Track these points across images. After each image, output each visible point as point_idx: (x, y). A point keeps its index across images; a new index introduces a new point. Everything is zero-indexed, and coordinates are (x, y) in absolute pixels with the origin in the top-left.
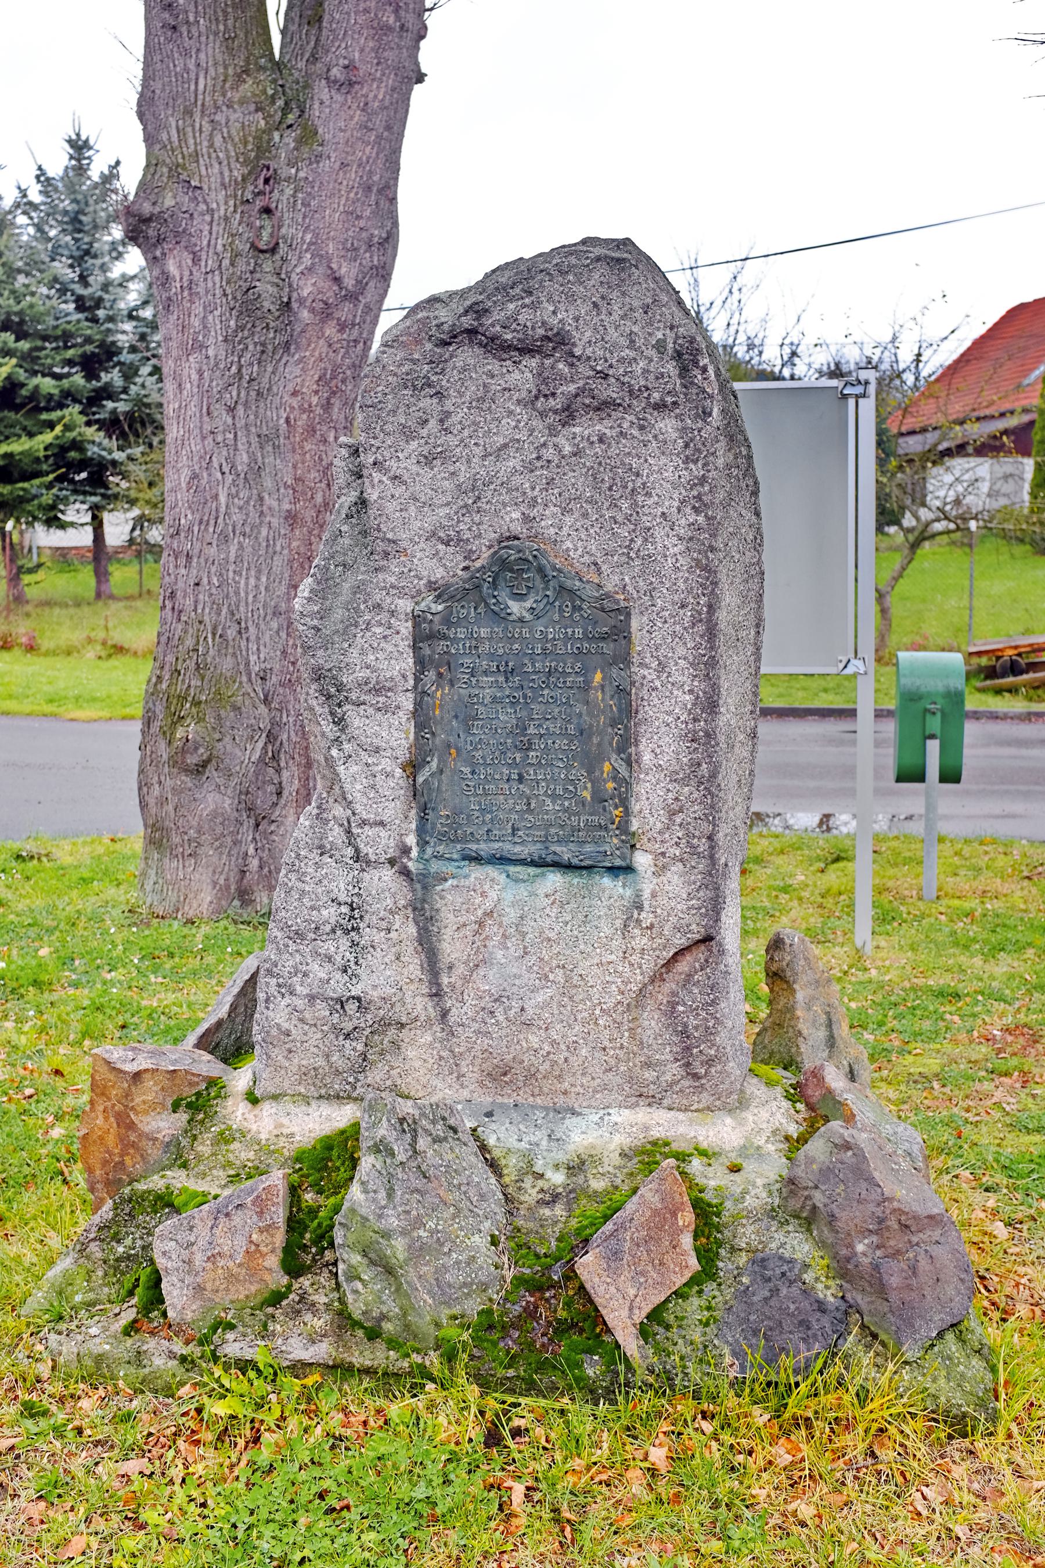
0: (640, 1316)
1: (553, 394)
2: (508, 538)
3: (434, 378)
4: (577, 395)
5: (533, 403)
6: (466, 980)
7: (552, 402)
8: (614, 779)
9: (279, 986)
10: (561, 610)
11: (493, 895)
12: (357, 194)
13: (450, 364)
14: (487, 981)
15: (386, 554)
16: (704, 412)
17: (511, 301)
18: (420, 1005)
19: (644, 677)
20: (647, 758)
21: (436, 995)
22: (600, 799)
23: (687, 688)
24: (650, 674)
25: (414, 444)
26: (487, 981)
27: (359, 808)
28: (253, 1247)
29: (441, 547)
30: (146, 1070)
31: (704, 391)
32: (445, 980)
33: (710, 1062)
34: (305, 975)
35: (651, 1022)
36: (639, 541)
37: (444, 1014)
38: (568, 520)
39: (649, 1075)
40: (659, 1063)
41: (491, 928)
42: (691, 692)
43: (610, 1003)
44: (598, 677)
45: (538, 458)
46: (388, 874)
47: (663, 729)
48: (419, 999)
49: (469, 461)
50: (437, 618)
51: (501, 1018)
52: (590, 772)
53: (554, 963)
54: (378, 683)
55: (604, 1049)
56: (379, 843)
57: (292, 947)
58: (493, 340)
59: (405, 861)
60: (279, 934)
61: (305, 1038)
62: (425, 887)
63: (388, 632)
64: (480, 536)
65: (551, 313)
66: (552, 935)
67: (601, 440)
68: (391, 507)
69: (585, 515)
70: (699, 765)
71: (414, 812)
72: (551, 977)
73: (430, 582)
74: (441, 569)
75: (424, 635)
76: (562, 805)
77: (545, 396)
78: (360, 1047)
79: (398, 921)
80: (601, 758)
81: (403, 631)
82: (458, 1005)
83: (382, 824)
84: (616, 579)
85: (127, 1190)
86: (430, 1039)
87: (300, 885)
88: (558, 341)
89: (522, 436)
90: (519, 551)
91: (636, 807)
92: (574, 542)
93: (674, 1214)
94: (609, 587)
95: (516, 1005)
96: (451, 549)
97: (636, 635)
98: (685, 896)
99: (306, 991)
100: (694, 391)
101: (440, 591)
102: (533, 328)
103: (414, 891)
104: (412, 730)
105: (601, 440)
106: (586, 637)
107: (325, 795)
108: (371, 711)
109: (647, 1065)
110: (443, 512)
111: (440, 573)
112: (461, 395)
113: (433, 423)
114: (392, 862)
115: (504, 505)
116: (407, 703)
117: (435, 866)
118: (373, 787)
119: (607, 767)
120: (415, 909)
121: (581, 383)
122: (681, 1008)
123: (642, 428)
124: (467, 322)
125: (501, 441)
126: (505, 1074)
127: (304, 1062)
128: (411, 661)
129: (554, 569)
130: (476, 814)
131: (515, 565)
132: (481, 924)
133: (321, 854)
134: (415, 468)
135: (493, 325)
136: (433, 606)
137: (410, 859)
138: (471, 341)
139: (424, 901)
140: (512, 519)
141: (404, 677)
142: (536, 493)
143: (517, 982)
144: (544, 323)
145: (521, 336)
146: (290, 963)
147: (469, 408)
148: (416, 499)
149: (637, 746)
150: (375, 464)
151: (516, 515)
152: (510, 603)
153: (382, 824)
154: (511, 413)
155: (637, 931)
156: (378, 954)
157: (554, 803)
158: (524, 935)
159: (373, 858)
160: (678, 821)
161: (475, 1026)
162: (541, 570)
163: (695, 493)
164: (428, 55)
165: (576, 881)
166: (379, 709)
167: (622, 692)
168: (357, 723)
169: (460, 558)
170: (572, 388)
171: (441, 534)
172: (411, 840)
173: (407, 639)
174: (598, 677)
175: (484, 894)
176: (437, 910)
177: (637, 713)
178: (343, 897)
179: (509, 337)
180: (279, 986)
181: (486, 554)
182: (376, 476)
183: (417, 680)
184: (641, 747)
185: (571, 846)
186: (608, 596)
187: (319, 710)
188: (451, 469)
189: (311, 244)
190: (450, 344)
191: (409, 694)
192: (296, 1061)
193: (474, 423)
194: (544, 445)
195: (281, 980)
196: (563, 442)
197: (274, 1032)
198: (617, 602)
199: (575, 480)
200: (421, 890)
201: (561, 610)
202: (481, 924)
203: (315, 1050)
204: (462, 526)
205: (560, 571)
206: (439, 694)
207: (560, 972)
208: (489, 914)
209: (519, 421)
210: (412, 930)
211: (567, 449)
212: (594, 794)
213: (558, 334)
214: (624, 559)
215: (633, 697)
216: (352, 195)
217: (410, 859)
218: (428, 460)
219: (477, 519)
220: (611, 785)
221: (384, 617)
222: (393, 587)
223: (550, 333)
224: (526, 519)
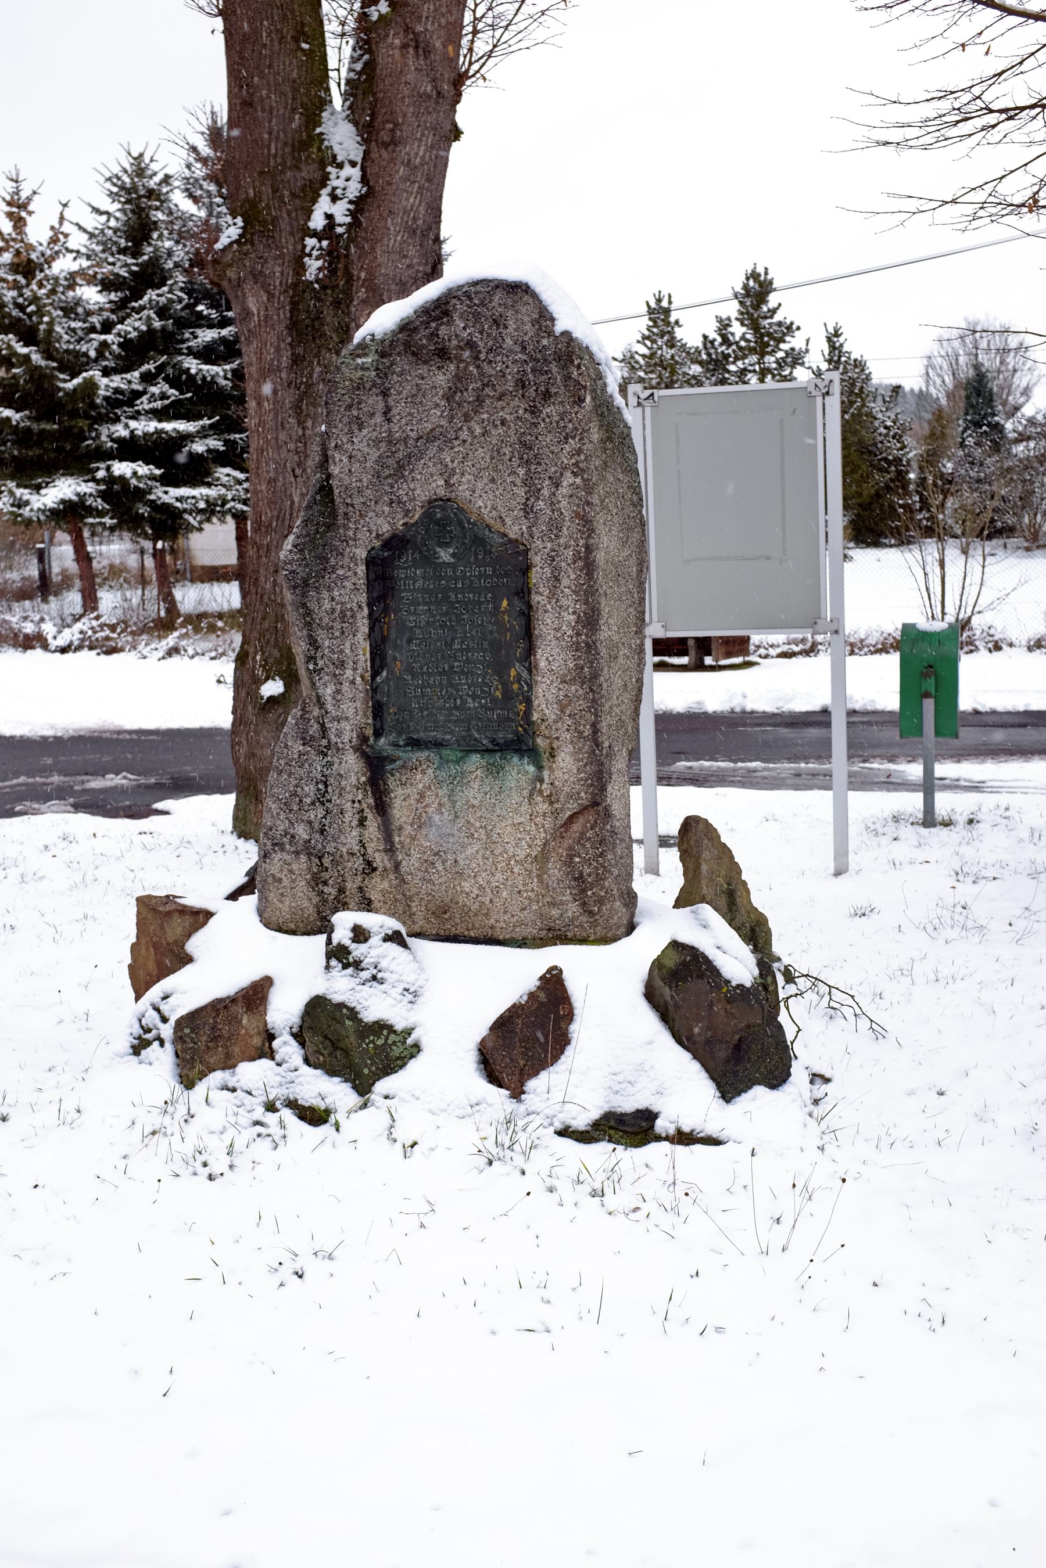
2: (436, 500)
12: (403, 236)
16: (579, 399)
19: (539, 602)
20: (543, 664)
23: (571, 610)
26: (429, 839)
31: (579, 383)
33: (601, 902)
35: (555, 871)
36: (532, 500)
37: (397, 866)
39: (555, 912)
40: (562, 903)
42: (574, 613)
43: (522, 854)
44: (505, 603)
51: (440, 868)
53: (478, 825)
55: (519, 892)
61: (293, 885)
66: (476, 802)
67: (503, 424)
70: (582, 668)
74: (387, 525)
76: (480, 703)
80: (508, 666)
91: (536, 703)
98: (575, 771)
100: (572, 384)
105: (503, 424)
109: (553, 904)
112: (400, 393)
119: (513, 673)
122: (577, 860)
123: (532, 412)
126: (445, 913)
127: (293, 904)
134: (366, 450)
135: (420, 339)
144: (457, 336)
147: (406, 403)
150: (336, 446)
155: (540, 799)
157: (474, 701)
160: (568, 712)
161: (420, 874)
163: (573, 461)
164: (463, 115)
174: (505, 603)
189: (365, 280)
193: (410, 414)
194: (461, 428)
203: (302, 894)
204: (401, 492)
216: (399, 238)
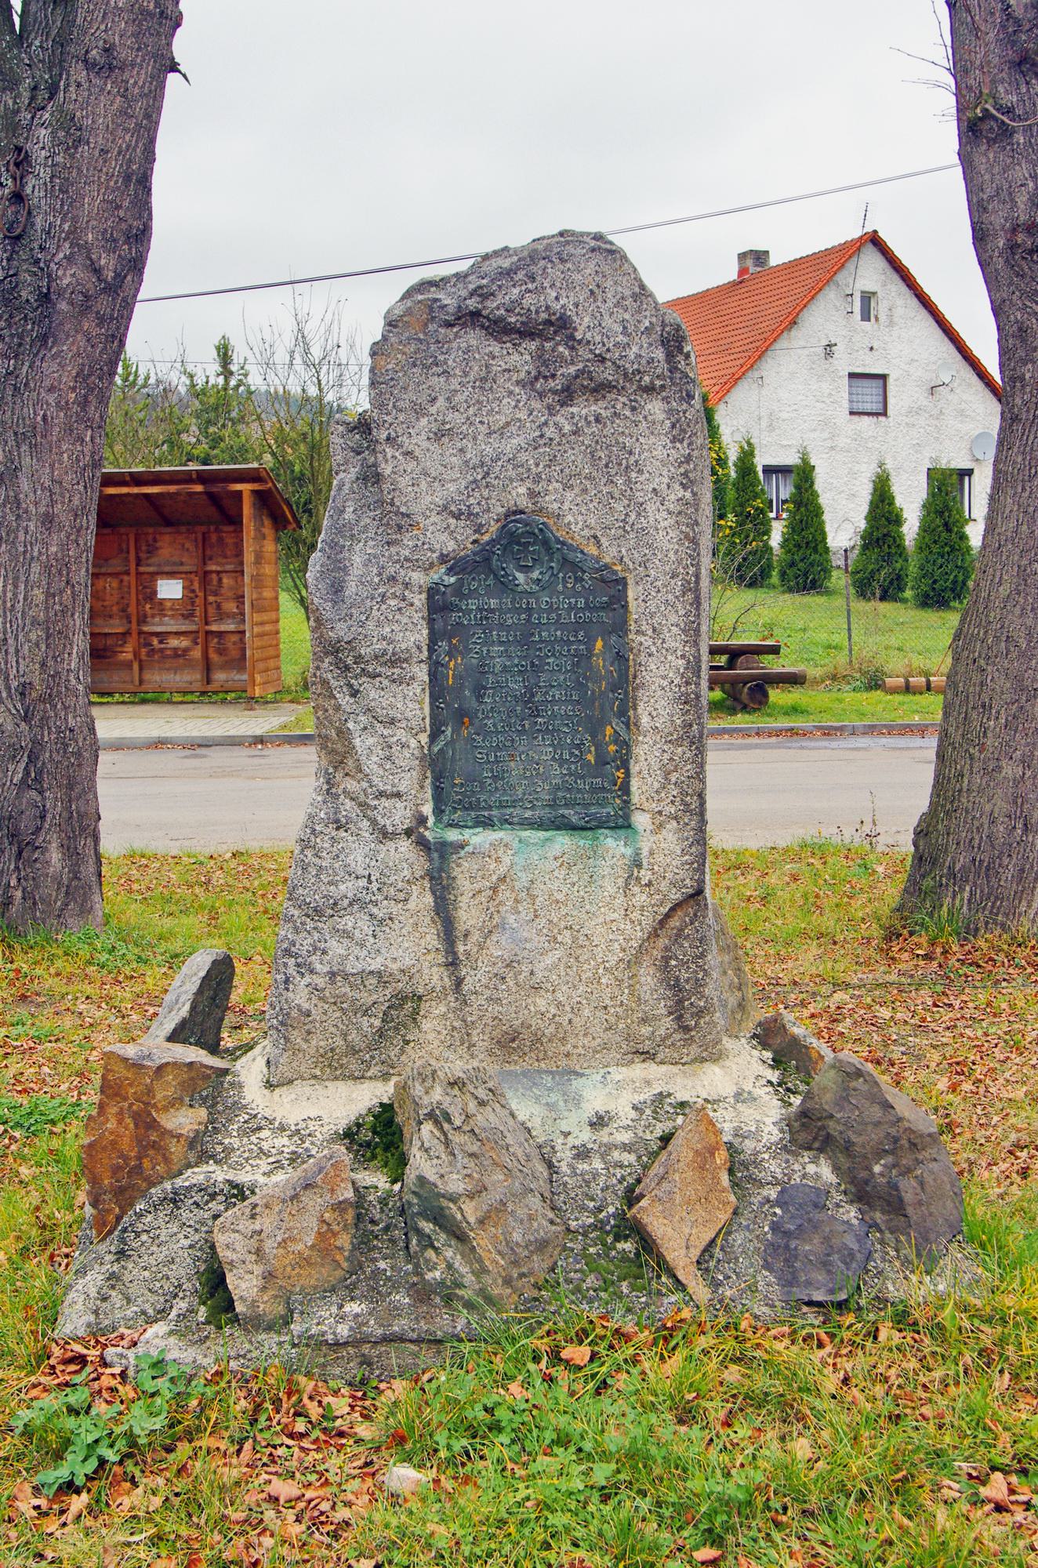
0: (695, 1253)
1: (553, 376)
2: (515, 513)
3: (441, 358)
4: (577, 377)
5: (532, 384)
6: (481, 947)
7: (551, 384)
8: (616, 742)
9: (298, 965)
10: (565, 582)
11: (506, 860)
12: (116, 182)
13: (454, 345)
14: (499, 948)
15: (400, 527)
16: (688, 395)
17: (514, 286)
18: (435, 976)
19: (641, 644)
20: (645, 720)
21: (451, 964)
22: (602, 761)
23: (679, 653)
24: (647, 641)
25: (424, 421)
26: (499, 948)
27: (376, 780)
28: (325, 1228)
29: (452, 521)
30: (168, 1064)
31: (687, 376)
32: (461, 948)
33: (700, 1013)
34: (324, 952)
35: (648, 978)
36: (633, 516)
37: (459, 983)
38: (569, 495)
39: (645, 1030)
40: (656, 1018)
41: (505, 894)
42: (683, 656)
43: (613, 960)
44: (599, 644)
45: (542, 436)
46: (405, 845)
47: (659, 693)
48: (435, 969)
49: (475, 439)
50: (449, 590)
51: (511, 983)
52: (594, 736)
53: (563, 924)
54: (394, 654)
55: (605, 1008)
56: (399, 815)
57: (310, 925)
58: (495, 322)
59: (422, 830)
60: (296, 913)
61: (325, 1018)
62: (442, 857)
63: (402, 604)
64: (488, 510)
65: (555, 298)
66: (560, 897)
67: (597, 420)
68: (403, 482)
69: (585, 491)
70: (691, 726)
71: (429, 781)
72: (560, 938)
73: (442, 555)
74: (452, 542)
75: (438, 604)
76: (569, 769)
77: (545, 377)
78: (377, 1023)
79: (415, 890)
80: (602, 722)
81: (417, 603)
82: (472, 973)
83: (398, 795)
84: (613, 551)
85: (168, 1186)
86: (444, 1009)
87: (318, 861)
88: (561, 325)
89: (522, 415)
90: (527, 525)
91: (634, 769)
92: (576, 517)
93: (712, 1154)
94: (607, 560)
95: (525, 968)
96: (462, 523)
97: (632, 605)
98: (679, 852)
99: (326, 969)
100: (678, 375)
101: (456, 565)
102: (537, 312)
103: (431, 860)
104: (427, 700)
105: (597, 420)
106: (587, 607)
107: (331, 770)
108: (386, 682)
109: (644, 1021)
110: (452, 487)
111: (451, 546)
112: (466, 374)
113: (441, 402)
114: (408, 833)
115: (511, 480)
116: (422, 673)
117: (453, 835)
118: (388, 758)
119: (609, 731)
120: (432, 879)
121: (581, 366)
122: (673, 963)
123: (633, 409)
124: (472, 304)
125: (503, 420)
126: (513, 1040)
127: (322, 1043)
128: (425, 632)
129: (558, 541)
130: (489, 781)
131: (524, 538)
132: (495, 889)
133: (338, 829)
134: (425, 444)
135: (498, 308)
136: (446, 578)
137: (427, 828)
138: (473, 324)
139: (441, 870)
140: (518, 495)
141: (419, 648)
142: (540, 469)
143: (528, 946)
144: (548, 308)
145: (524, 319)
146: (309, 941)
147: (474, 388)
148: (426, 474)
149: (635, 709)
150: (388, 439)
151: (522, 490)
152: (517, 574)
153: (398, 795)
154: (511, 393)
155: (636, 889)
156: (396, 925)
157: (561, 766)
158: (534, 898)
159: (390, 829)
160: (673, 780)
161: (487, 993)
162: (546, 543)
163: (682, 470)
165: (581, 843)
166: (394, 681)
167: (621, 658)
168: (373, 694)
169: (470, 532)
170: (572, 370)
171: (453, 508)
172: (427, 809)
173: (421, 610)
174: (599, 644)
175: (498, 860)
176: (454, 878)
177: (635, 677)
178: (360, 871)
179: (513, 320)
180: (298, 965)
181: (494, 528)
182: (389, 452)
183: (431, 650)
184: (640, 711)
185: (578, 809)
186: (606, 566)
187: (334, 683)
188: (459, 445)
190: (452, 326)
191: (423, 665)
192: (314, 1043)
193: (478, 401)
194: (546, 424)
195: (300, 960)
196: (562, 420)
197: (294, 1013)
198: (615, 573)
199: (575, 457)
200: (439, 861)
201: (565, 582)
202: (495, 889)
203: (333, 1030)
204: (472, 501)
205: (563, 543)
206: (452, 664)
207: (567, 933)
208: (502, 879)
209: (518, 401)
210: (429, 899)
211: (567, 428)
212: (598, 757)
213: (561, 318)
214: (621, 531)
215: (631, 663)
216: (112, 183)
217: (427, 828)
218: (439, 435)
219: (486, 493)
220: (612, 748)
221: (398, 589)
222: (407, 559)
223: (553, 318)
224: (532, 494)
